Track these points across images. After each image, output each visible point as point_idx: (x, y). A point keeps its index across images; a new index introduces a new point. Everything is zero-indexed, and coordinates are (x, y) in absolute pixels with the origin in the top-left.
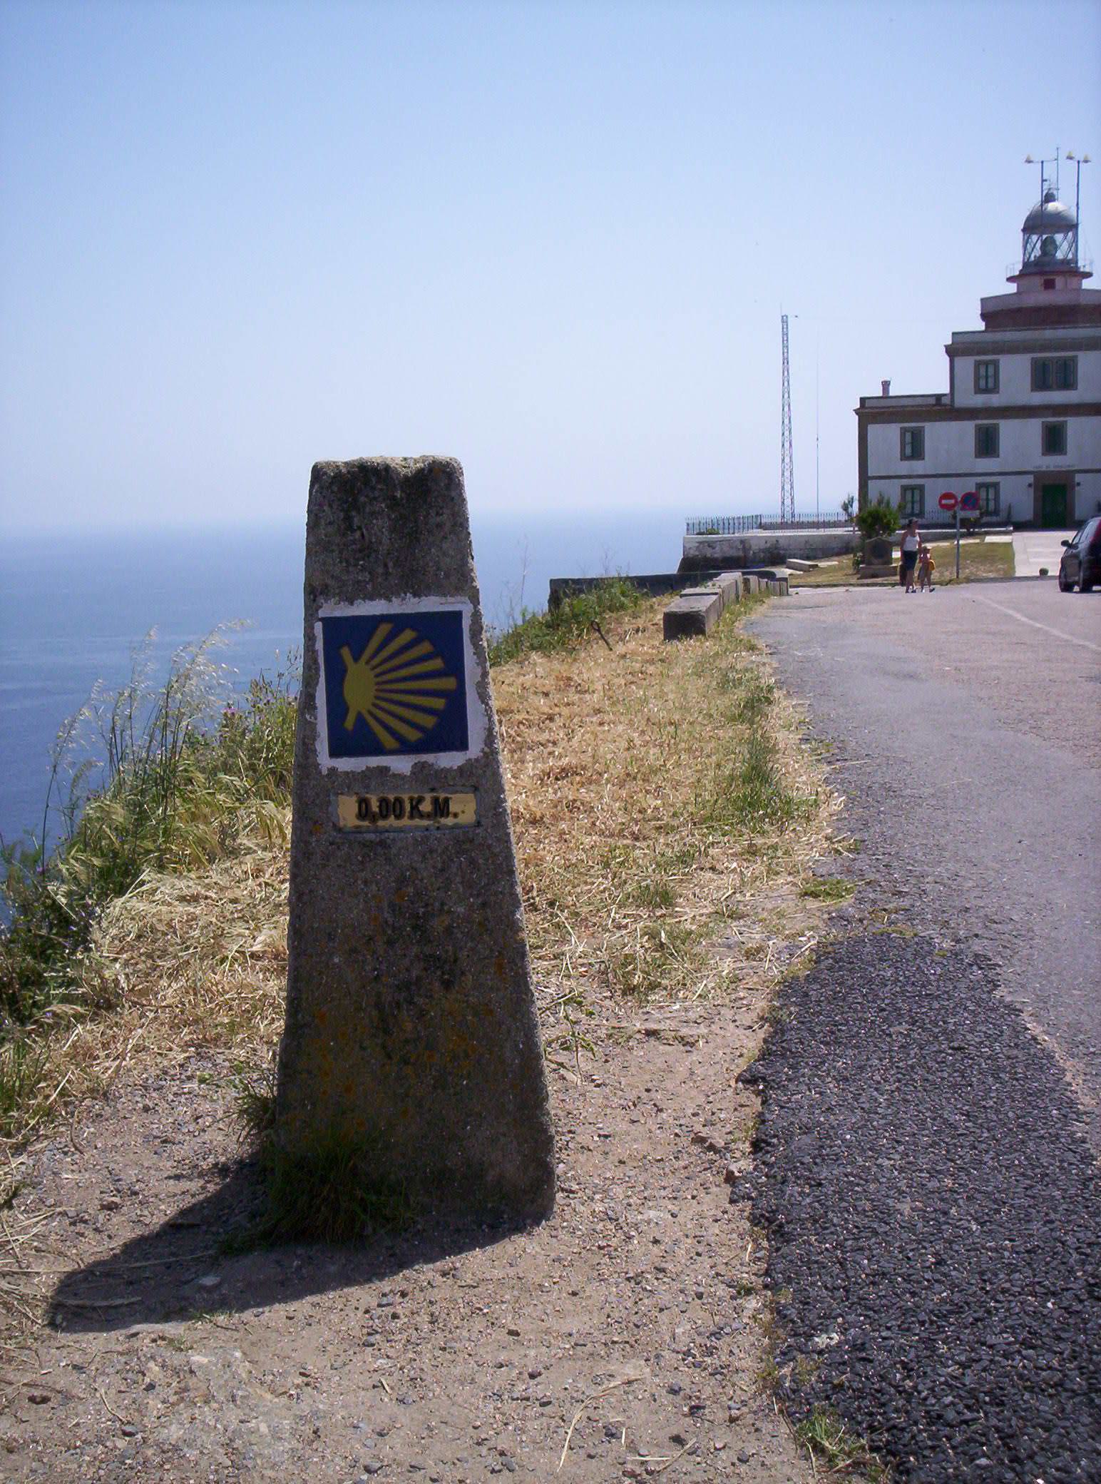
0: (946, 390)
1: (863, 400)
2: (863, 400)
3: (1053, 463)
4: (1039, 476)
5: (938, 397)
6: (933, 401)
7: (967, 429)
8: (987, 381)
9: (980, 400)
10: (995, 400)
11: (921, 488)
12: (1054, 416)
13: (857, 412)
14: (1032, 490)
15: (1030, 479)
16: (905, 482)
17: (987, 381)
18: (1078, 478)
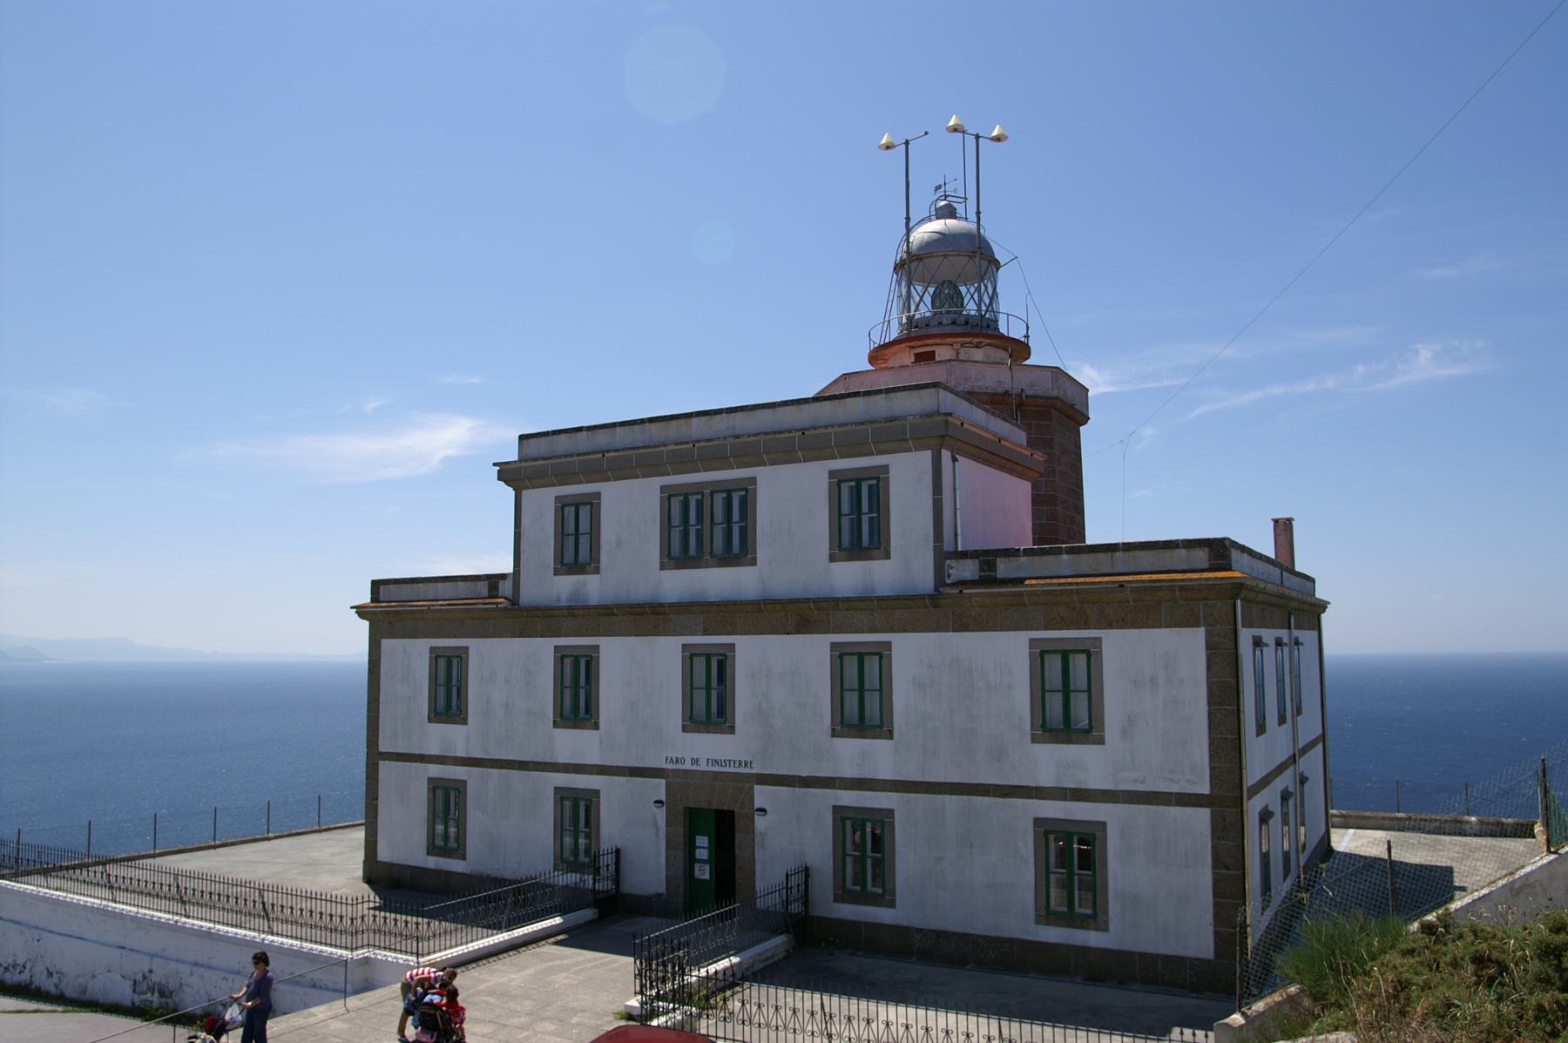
0: (507, 566)
1: (376, 585)
2: (376, 585)
3: (706, 751)
4: (677, 779)
5: (493, 580)
6: (483, 588)
7: (535, 657)
8: (577, 543)
9: (563, 587)
10: (594, 588)
11: (460, 787)
12: (706, 633)
13: (361, 611)
14: (661, 814)
15: (659, 788)
16: (436, 771)
17: (577, 543)
18: (762, 795)
